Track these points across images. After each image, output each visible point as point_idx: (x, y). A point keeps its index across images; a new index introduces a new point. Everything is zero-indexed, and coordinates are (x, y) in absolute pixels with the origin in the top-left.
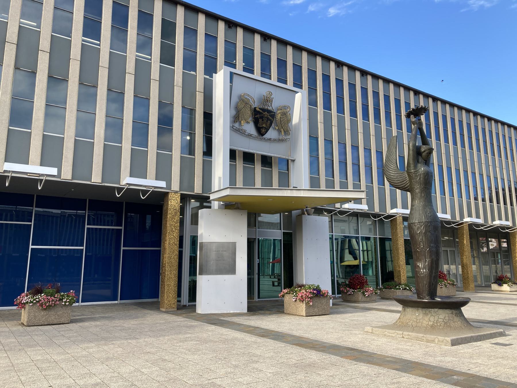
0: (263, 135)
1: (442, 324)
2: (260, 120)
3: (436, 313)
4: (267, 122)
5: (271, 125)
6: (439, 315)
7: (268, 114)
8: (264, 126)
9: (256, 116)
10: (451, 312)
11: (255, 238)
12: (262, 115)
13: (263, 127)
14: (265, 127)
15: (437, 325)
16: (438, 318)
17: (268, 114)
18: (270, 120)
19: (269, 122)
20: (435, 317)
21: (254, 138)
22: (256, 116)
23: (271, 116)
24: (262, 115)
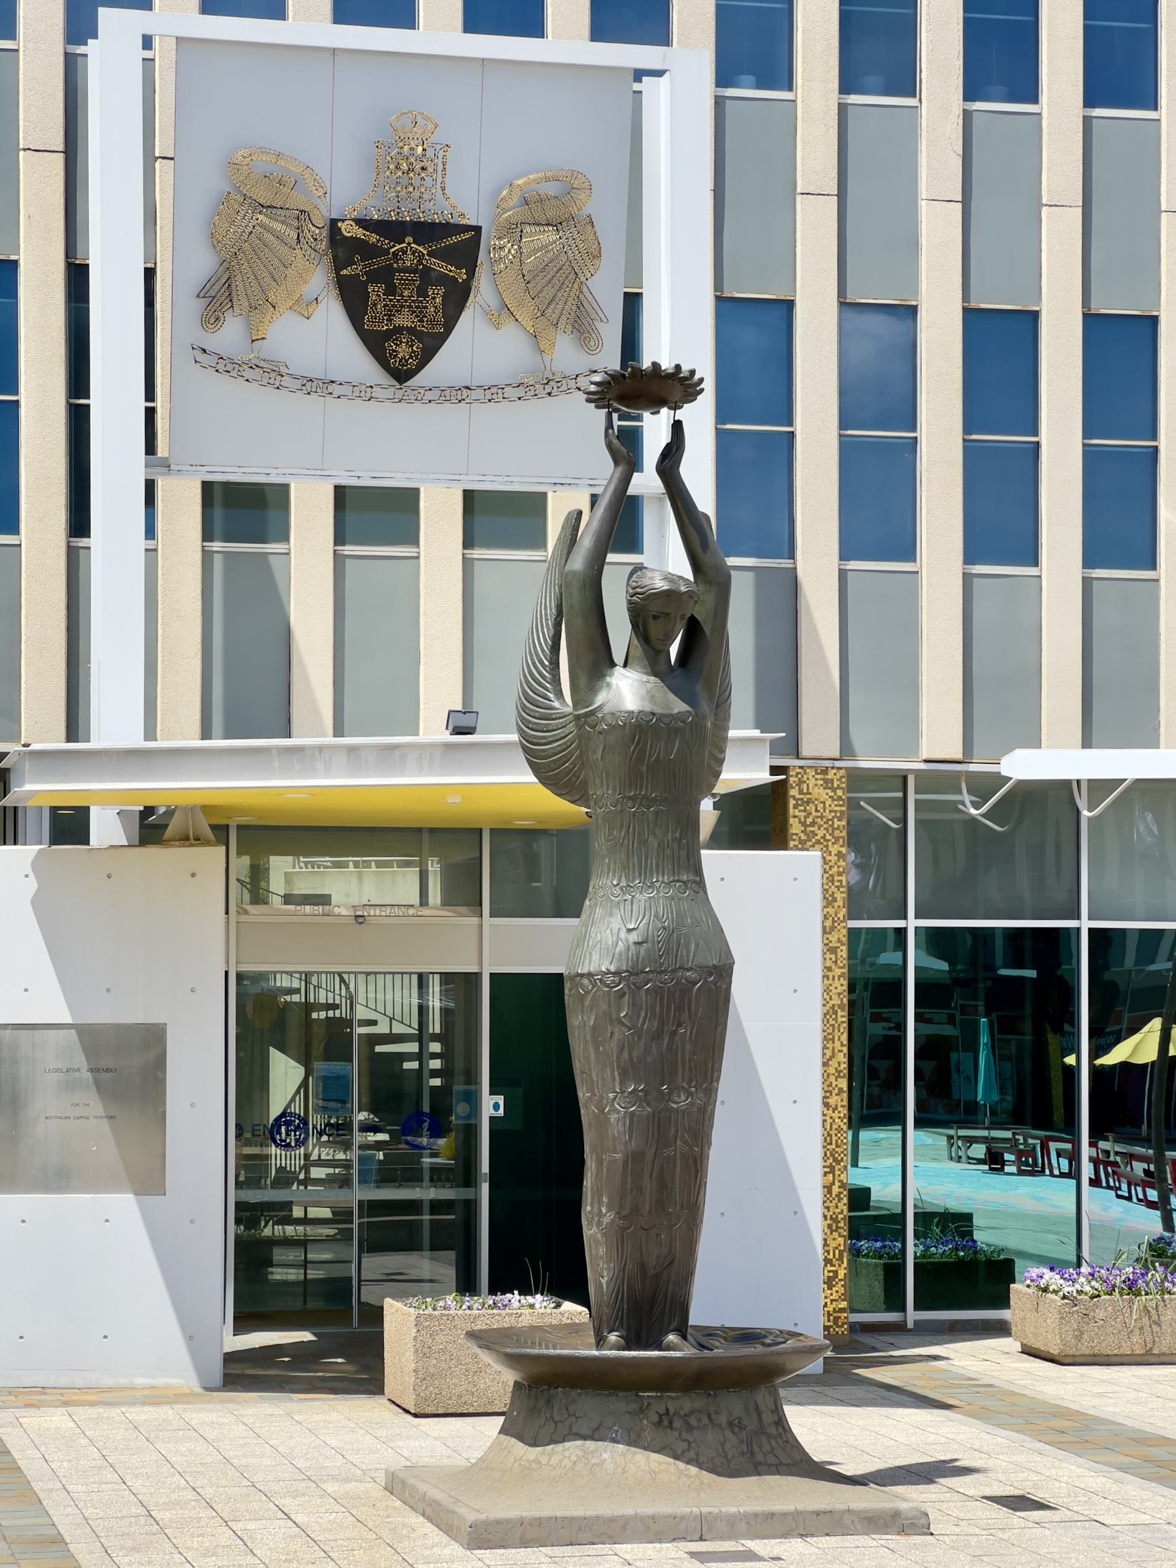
0: (401, 375)
1: (569, 1457)
2: (375, 291)
3: (570, 1408)
4: (422, 292)
5: (458, 297)
6: (577, 1418)
7: (420, 249)
8: (404, 320)
9: (344, 272)
10: (634, 1406)
11: (473, 969)
12: (381, 261)
13: (399, 330)
14: (411, 331)
15: (549, 1460)
16: (567, 1431)
17: (420, 249)
18: (444, 280)
19: (437, 294)
20: (560, 1425)
21: (366, 394)
22: (344, 272)
23: (446, 255)
24: (381, 261)
